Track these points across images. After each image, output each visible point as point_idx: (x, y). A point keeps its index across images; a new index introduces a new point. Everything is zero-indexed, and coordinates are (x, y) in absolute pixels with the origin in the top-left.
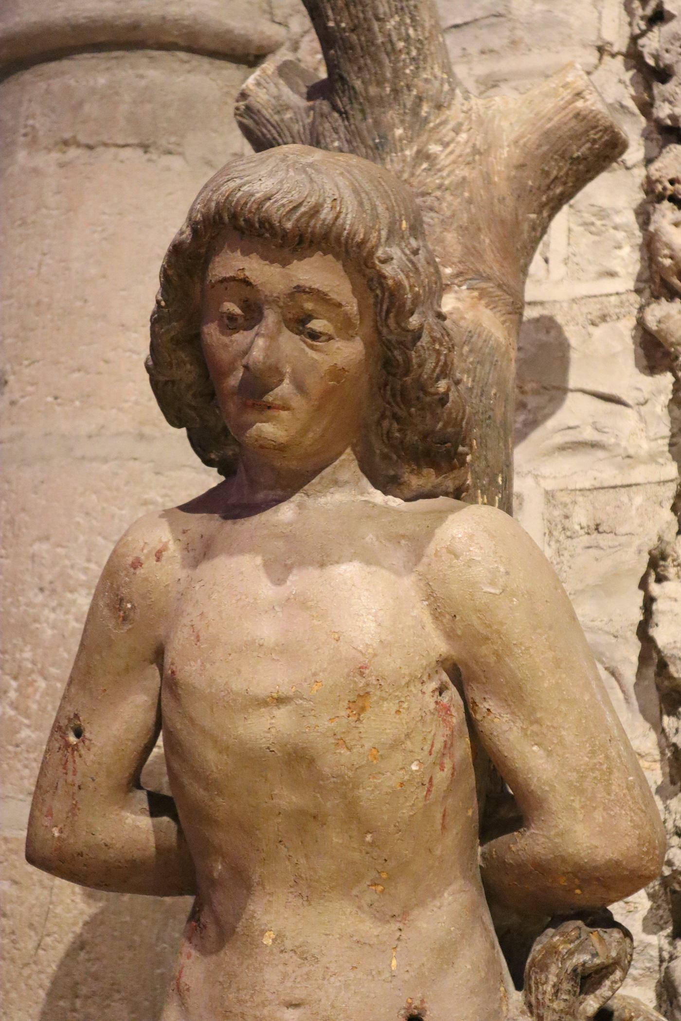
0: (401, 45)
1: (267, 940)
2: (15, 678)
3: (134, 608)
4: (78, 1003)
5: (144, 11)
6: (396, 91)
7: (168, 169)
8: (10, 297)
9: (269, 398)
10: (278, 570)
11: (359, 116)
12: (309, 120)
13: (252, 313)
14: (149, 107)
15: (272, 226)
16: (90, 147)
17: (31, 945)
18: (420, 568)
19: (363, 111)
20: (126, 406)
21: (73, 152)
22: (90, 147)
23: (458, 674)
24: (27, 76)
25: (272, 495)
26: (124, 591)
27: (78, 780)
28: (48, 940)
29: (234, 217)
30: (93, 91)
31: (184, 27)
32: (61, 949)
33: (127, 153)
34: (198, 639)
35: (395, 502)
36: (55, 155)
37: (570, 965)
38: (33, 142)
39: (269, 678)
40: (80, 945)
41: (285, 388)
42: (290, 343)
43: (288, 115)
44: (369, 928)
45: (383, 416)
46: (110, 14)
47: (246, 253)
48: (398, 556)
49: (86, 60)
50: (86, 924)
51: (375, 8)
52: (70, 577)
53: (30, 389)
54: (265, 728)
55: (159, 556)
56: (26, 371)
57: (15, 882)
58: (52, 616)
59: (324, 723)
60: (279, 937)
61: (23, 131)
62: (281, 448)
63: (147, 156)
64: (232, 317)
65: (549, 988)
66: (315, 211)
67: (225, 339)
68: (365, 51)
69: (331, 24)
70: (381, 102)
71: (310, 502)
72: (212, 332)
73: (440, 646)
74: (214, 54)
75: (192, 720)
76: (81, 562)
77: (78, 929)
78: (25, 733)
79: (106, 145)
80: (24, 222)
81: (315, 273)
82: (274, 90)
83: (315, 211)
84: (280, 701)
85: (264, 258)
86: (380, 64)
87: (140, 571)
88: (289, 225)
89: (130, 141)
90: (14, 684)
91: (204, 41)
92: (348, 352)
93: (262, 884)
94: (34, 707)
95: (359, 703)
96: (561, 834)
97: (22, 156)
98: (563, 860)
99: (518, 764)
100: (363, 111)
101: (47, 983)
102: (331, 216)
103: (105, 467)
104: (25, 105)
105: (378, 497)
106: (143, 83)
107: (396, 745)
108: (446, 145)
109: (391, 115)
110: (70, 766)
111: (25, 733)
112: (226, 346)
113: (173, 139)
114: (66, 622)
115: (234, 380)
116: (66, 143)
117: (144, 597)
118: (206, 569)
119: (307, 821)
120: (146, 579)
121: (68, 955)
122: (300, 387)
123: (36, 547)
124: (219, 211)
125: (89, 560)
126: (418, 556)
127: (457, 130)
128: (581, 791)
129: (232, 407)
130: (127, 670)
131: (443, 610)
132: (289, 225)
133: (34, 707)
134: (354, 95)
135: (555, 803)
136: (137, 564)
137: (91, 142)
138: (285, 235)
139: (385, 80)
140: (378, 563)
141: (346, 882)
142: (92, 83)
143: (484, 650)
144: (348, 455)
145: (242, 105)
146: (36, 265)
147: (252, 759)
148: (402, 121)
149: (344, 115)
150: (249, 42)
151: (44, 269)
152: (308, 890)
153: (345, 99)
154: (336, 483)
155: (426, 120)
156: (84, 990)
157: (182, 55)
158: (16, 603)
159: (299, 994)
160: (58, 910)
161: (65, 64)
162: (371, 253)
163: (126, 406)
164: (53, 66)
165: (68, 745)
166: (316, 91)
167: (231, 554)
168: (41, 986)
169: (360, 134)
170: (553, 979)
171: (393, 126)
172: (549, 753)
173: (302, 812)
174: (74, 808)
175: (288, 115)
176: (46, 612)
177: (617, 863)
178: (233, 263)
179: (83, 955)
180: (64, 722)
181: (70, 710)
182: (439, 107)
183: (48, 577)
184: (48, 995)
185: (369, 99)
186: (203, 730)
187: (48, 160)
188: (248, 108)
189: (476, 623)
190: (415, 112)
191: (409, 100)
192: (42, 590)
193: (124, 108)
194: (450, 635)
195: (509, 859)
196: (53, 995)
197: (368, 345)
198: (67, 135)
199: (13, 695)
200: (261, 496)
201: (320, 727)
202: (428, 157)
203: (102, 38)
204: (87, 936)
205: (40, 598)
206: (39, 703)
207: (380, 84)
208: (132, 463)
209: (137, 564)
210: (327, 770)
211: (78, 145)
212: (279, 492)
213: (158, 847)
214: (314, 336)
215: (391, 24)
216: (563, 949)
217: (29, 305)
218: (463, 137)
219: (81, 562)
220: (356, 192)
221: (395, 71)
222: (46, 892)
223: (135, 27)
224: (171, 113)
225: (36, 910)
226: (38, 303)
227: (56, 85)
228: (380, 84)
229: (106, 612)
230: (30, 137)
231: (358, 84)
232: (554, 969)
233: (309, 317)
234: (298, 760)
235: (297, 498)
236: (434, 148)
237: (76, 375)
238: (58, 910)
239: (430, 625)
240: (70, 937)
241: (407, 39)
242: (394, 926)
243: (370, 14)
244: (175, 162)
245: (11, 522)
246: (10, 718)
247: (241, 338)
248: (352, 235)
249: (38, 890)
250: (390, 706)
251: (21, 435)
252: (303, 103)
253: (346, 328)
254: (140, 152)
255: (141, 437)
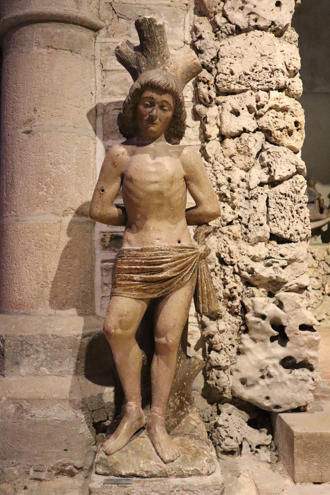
0: (160, 43)
1: (151, 228)
2: (46, 186)
3: (117, 164)
4: (67, 260)
5: (71, 14)
6: (159, 53)
7: (77, 58)
8: (36, 87)
9: (155, 122)
10: (154, 157)
11: (150, 58)
12: (136, 56)
13: (152, 105)
14: (71, 40)
15: (160, 88)
16: (56, 49)
17: (55, 247)
18: (180, 158)
19: (151, 57)
20: (70, 119)
21: (51, 50)
22: (56, 49)
23: (186, 179)
24: (35, 26)
25: (148, 142)
26: (115, 161)
27: (104, 200)
28: (59, 246)
29: (152, 84)
30: (56, 33)
31: (82, 20)
32: (63, 248)
33: (66, 52)
34: (137, 170)
35: (171, 145)
36: (45, 50)
37: (204, 232)
38: (38, 44)
39: (154, 178)
40: (67, 247)
41: (157, 120)
42: (160, 111)
43: (130, 54)
44: (171, 226)
45: (170, 127)
46: (62, 14)
47: (153, 92)
48: (175, 155)
49: (54, 24)
50: (68, 242)
51: (156, 34)
52: (59, 161)
53: (43, 112)
54: (153, 188)
55: (123, 154)
56: (42, 108)
57: (50, 233)
58: (55, 170)
59: (166, 187)
60: (154, 228)
61: (35, 41)
62: (155, 132)
63: (72, 53)
64: (147, 105)
65: (201, 236)
66: (168, 85)
67: (145, 109)
68: (153, 43)
69: (145, 35)
70: (155, 55)
71: (156, 144)
72: (141, 107)
73: (184, 173)
74: (87, 27)
75: (136, 186)
76: (61, 157)
77: (66, 243)
78: (49, 199)
79: (61, 49)
80: (38, 67)
81: (167, 98)
82: (126, 47)
83: (168, 85)
84: (156, 182)
85: (157, 93)
86: (156, 46)
87: (119, 157)
88: (164, 88)
89: (67, 49)
90: (45, 187)
91: (85, 24)
92: (169, 114)
93: (150, 218)
94: (52, 192)
95: (172, 183)
96: (205, 208)
97: (35, 48)
98: (205, 213)
99: (197, 196)
100: (151, 57)
101: (60, 256)
102: (171, 87)
103: (66, 134)
104: (35, 34)
105: (167, 143)
106: (70, 33)
107: (178, 191)
108: (169, 67)
109: (157, 59)
110: (102, 197)
111: (49, 199)
112: (145, 111)
113: (78, 50)
114: (59, 172)
115: (146, 118)
116: (49, 47)
117: (120, 162)
118: (135, 157)
119: (160, 206)
120: (120, 158)
121: (64, 249)
122: (160, 120)
123: (49, 153)
124: (148, 83)
125: (63, 157)
126: (180, 156)
127: (171, 64)
128: (209, 200)
129: (145, 123)
130: (115, 177)
131: (185, 166)
132: (164, 88)
133: (52, 192)
134: (149, 53)
135: (204, 202)
136: (118, 155)
137: (57, 48)
138: (163, 89)
139: (156, 50)
140: (172, 157)
141: (167, 217)
142: (56, 31)
143: (192, 174)
144: (163, 135)
145: (117, 49)
146: (43, 80)
147: (150, 194)
148: (160, 61)
149: (146, 57)
150: (96, 25)
151: (45, 81)
152: (159, 218)
153: (147, 53)
154: (161, 140)
155: (165, 61)
156: (69, 257)
157: (79, 26)
158: (44, 167)
159: (159, 237)
160: (62, 239)
161: (47, 24)
162: (178, 95)
163: (70, 119)
164: (43, 24)
165: (101, 193)
166: (136, 49)
167: (142, 153)
168: (58, 256)
169: (150, 61)
170: (201, 235)
171: (157, 61)
172: (203, 193)
173: (160, 204)
174: (103, 206)
175: (130, 54)
176: (53, 169)
177: (215, 213)
178: (149, 94)
179: (68, 249)
180: (99, 188)
181: (100, 186)
182: (167, 58)
183: (53, 161)
184: (60, 258)
185: (152, 54)
186: (139, 188)
187: (44, 51)
188: (119, 51)
189: (191, 168)
190: (163, 59)
191: (161, 55)
192: (51, 164)
193: (65, 39)
194: (186, 171)
195: (193, 214)
196: (61, 258)
197: (173, 113)
198: (49, 45)
199: (45, 190)
200: (146, 142)
201: (165, 187)
202: (165, 69)
203: (59, 19)
204: (69, 245)
205: (51, 166)
206: (53, 192)
207: (155, 51)
208: (73, 134)
209: (118, 155)
210: (166, 195)
211: (53, 48)
212: (150, 141)
213: (119, 215)
214: (164, 110)
215: (159, 38)
216: (204, 229)
217: (42, 90)
218: (172, 65)
219: (61, 157)
220: (175, 82)
221: (159, 48)
222: (58, 235)
223: (69, 18)
224: (77, 42)
225: (56, 239)
226: (44, 90)
227: (45, 30)
228: (155, 51)
229: (110, 165)
230: (37, 43)
231: (150, 50)
232: (202, 233)
233: (164, 106)
234: (160, 194)
235: (154, 143)
236: (167, 68)
237: (57, 110)
238: (62, 239)
239: (182, 169)
240: (64, 245)
241: (162, 42)
242: (175, 225)
243: (155, 35)
244: (79, 56)
245: (42, 147)
246: (45, 195)
247: (149, 109)
248: (175, 91)
249: (56, 235)
250: (177, 184)
251: (42, 125)
252: (133, 52)
253: (170, 109)
254: (70, 52)
255: (75, 127)
